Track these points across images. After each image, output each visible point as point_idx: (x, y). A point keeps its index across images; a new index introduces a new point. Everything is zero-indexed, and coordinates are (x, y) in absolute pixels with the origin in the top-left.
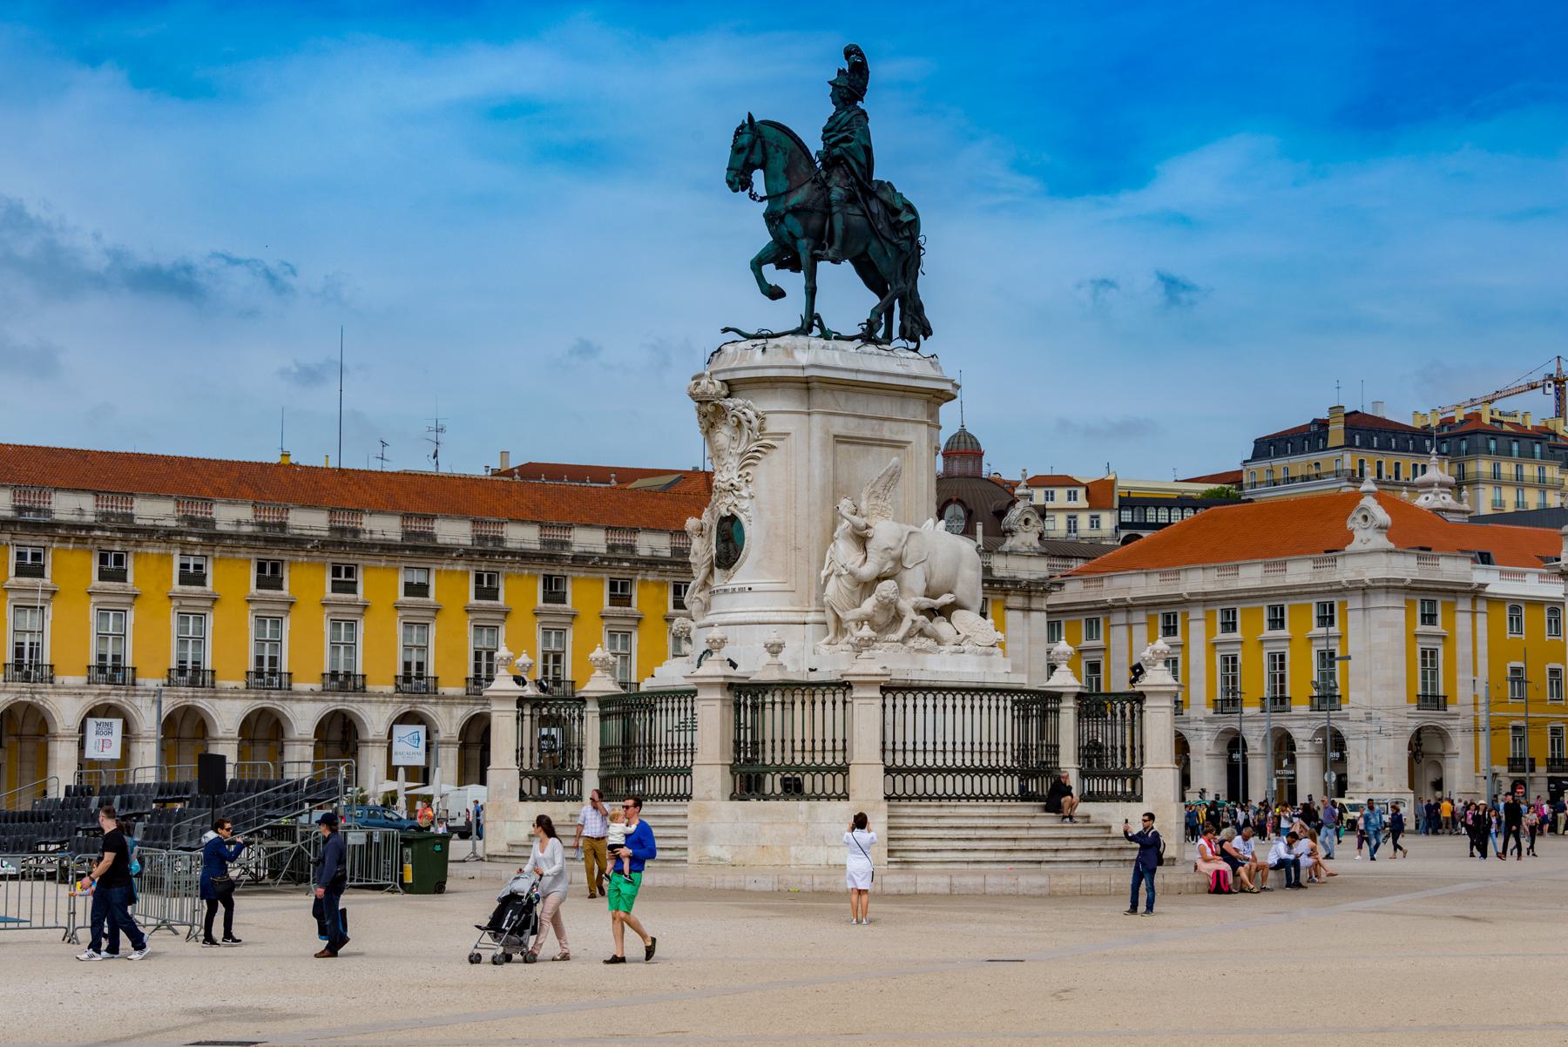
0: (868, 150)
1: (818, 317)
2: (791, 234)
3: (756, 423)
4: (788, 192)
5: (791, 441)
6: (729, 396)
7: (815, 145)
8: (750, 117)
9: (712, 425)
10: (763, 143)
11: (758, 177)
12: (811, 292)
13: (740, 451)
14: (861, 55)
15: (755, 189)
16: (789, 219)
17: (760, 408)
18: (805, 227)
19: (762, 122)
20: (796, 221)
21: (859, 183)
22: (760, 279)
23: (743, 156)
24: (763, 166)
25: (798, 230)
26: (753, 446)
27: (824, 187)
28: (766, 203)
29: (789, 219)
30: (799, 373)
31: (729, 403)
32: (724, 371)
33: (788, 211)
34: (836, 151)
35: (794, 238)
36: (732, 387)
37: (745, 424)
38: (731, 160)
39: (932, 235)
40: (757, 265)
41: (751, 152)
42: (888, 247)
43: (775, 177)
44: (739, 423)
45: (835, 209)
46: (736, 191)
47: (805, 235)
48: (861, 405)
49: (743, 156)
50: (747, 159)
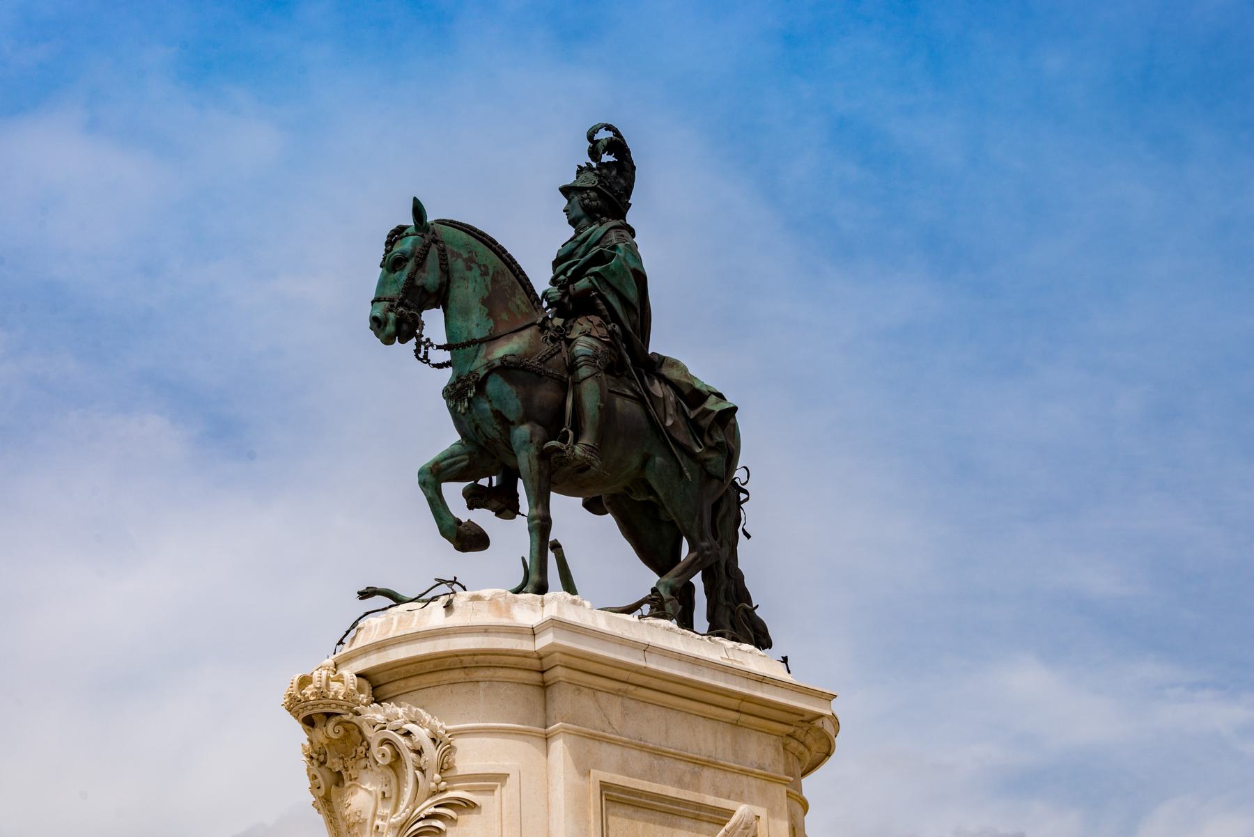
0: (641, 279)
1: (556, 547)
2: (498, 414)
3: (432, 754)
4: (492, 339)
5: (507, 792)
6: (378, 700)
7: (541, 280)
8: (418, 211)
9: (339, 779)
10: (443, 252)
11: (434, 323)
12: (542, 526)
13: (396, 819)
14: (618, 146)
15: (426, 333)
16: (496, 386)
17: (442, 726)
18: (527, 401)
19: (442, 222)
20: (507, 388)
21: (626, 337)
22: (438, 505)
23: (402, 276)
24: (440, 298)
25: (513, 407)
26: (427, 807)
27: (562, 338)
28: (449, 372)
29: (496, 386)
30: (526, 645)
31: (375, 714)
32: (365, 651)
33: (492, 370)
34: (583, 283)
35: (506, 424)
36: (378, 685)
37: (409, 757)
38: (382, 284)
39: (760, 462)
40: (434, 477)
41: (420, 265)
42: (684, 462)
43: (465, 312)
44: (397, 756)
45: (584, 372)
46: (388, 341)
48: (654, 726)
49: (402, 276)
50: (411, 279)
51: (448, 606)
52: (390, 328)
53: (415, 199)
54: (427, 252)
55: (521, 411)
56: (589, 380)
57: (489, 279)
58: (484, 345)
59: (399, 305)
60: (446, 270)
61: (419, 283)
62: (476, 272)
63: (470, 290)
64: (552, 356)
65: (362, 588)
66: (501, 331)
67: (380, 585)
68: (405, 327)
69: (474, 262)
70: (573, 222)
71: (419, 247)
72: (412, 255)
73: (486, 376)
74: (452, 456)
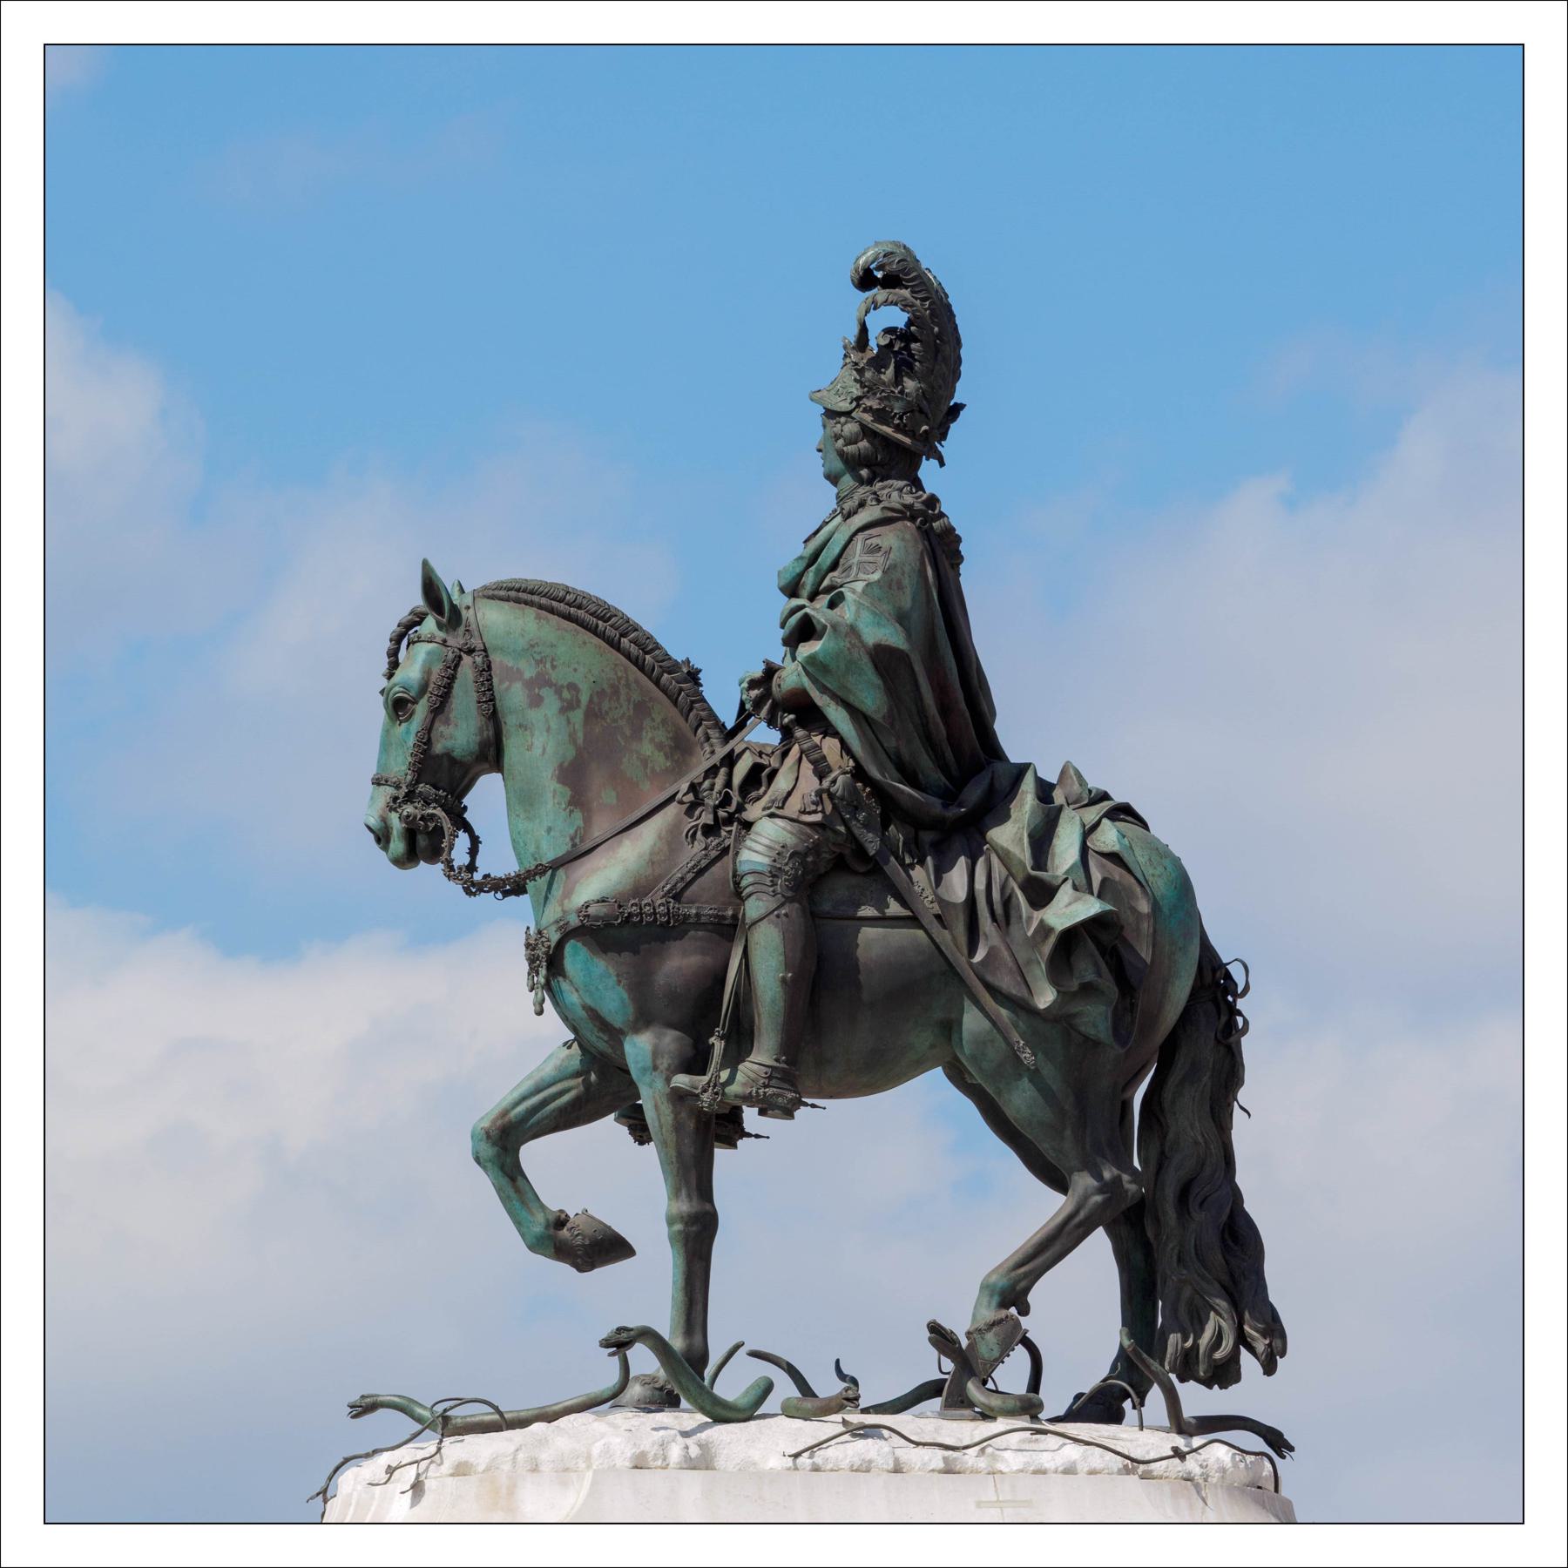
2: (594, 1015)
4: (577, 855)
10: (486, 669)
16: (576, 958)
18: (639, 987)
25: (614, 1002)
41: (440, 709)
45: (754, 908)
47: (643, 1019)
51: (417, 1488)
52: (398, 846)
53: (425, 564)
54: (452, 678)
55: (631, 1010)
56: (763, 925)
57: (578, 716)
58: (561, 873)
59: (410, 797)
60: (493, 717)
61: (438, 748)
62: (551, 704)
63: (537, 751)
64: (701, 872)
65: (354, 1397)
66: (597, 833)
67: (385, 1391)
68: (422, 841)
69: (549, 683)
70: (833, 479)
71: (437, 668)
72: (423, 689)
73: (560, 945)
74: (538, 1090)
